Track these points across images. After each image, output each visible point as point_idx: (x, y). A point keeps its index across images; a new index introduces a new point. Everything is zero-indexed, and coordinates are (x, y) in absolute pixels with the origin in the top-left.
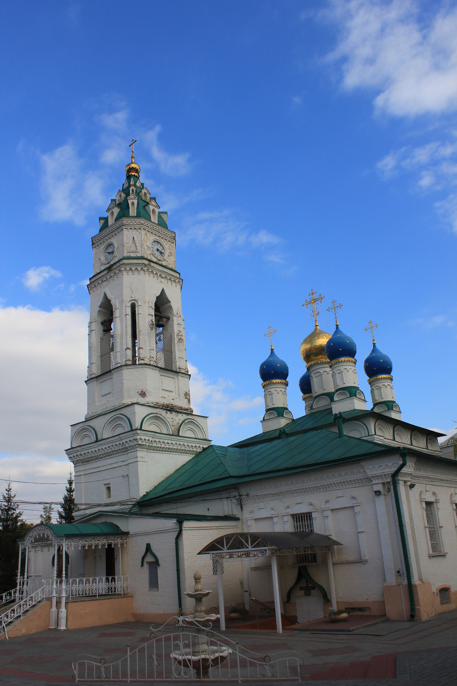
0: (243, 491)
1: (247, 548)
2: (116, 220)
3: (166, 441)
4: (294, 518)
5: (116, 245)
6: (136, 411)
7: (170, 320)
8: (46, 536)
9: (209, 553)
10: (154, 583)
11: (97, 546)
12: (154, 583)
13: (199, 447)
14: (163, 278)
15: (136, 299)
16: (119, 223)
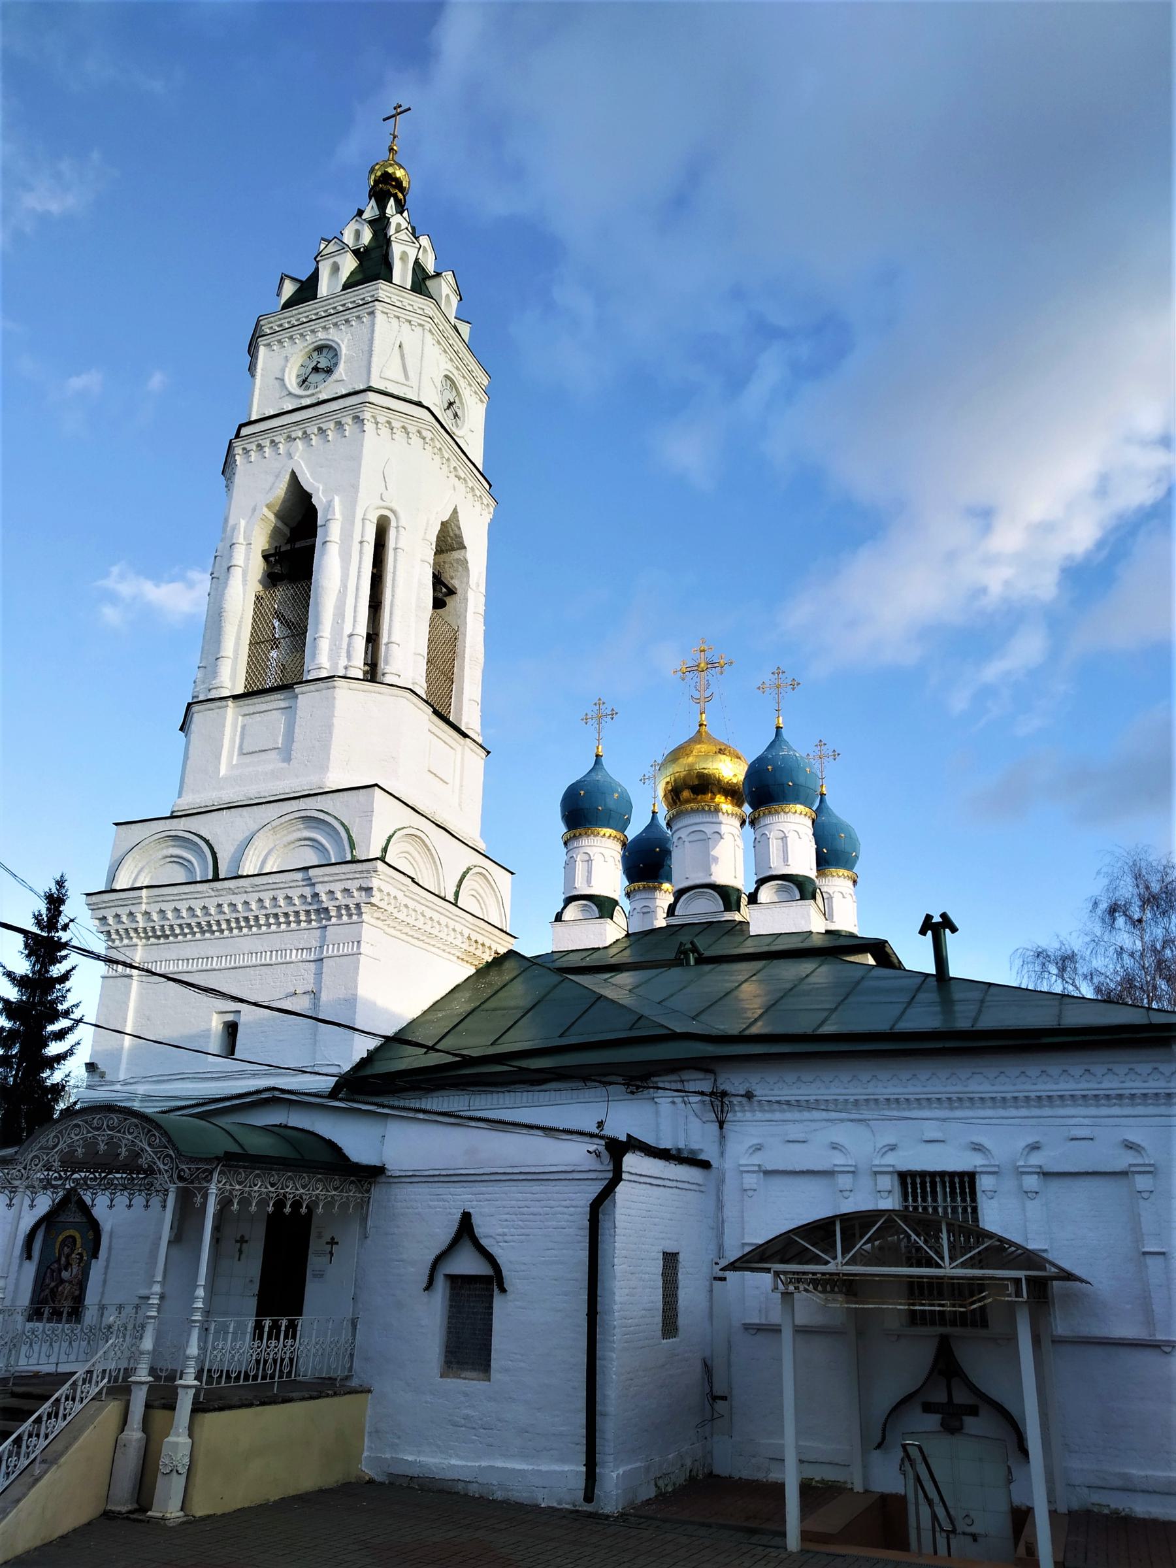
0: (734, 1082)
1: (938, 1266)
2: (346, 287)
3: (429, 913)
4: (903, 1185)
5: (344, 351)
6: (376, 806)
7: (457, 598)
8: (124, 1152)
9: (768, 1270)
10: (468, 1347)
11: (245, 1202)
12: (468, 1347)
13: (490, 948)
14: (459, 478)
15: (394, 506)
16: (364, 292)
